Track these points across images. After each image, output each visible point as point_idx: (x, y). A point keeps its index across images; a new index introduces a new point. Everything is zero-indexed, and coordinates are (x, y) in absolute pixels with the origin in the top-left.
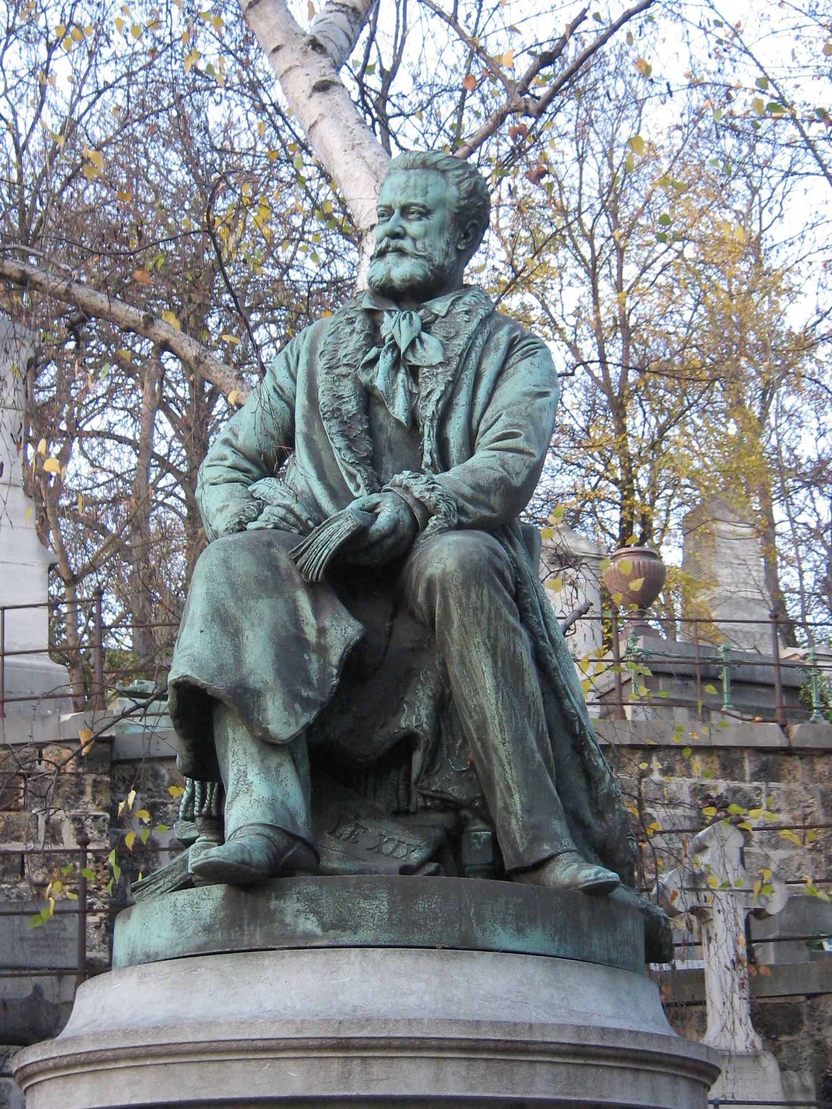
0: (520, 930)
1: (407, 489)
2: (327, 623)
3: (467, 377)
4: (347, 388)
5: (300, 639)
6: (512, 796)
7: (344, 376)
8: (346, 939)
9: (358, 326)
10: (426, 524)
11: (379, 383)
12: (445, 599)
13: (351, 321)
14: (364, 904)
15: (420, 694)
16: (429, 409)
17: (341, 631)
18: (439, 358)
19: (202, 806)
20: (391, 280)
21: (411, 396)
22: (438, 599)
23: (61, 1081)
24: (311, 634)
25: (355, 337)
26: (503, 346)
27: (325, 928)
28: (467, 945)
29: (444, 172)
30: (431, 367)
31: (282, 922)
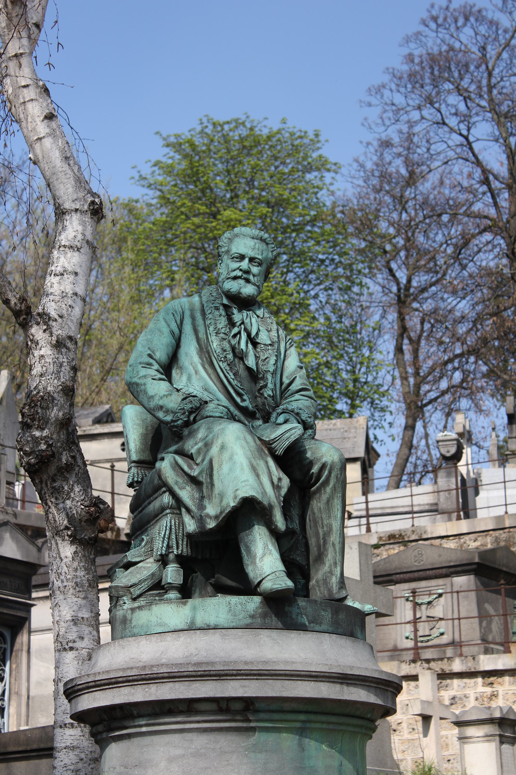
6: (336, 567)
8: (317, 628)
9: (223, 313)
13: (217, 309)
14: (323, 613)
15: (293, 512)
18: (269, 342)
19: (178, 548)
20: (240, 293)
22: (326, 473)
23: (187, 683)
29: (267, 244)
30: (265, 345)
31: (291, 617)
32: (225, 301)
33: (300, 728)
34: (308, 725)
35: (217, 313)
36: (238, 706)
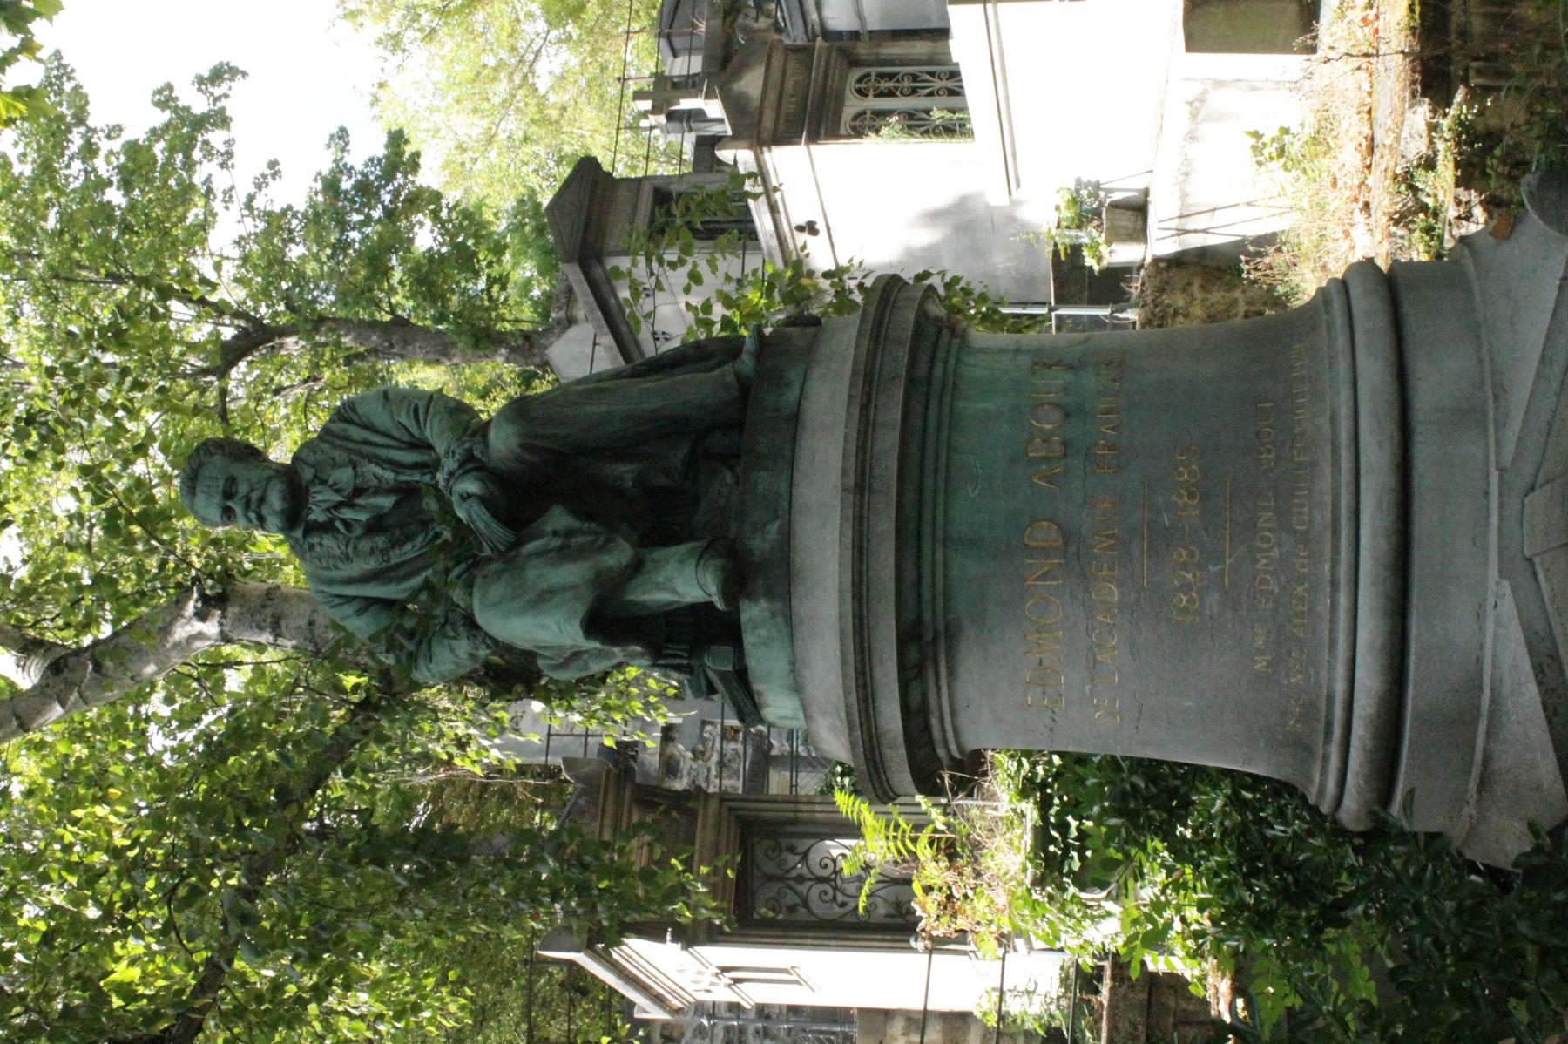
0: (787, 385)
1: (451, 474)
2: (549, 529)
3: (365, 449)
4: (365, 545)
5: (560, 549)
7: (355, 548)
9: (316, 540)
10: (479, 461)
11: (363, 517)
12: (536, 436)
13: (312, 547)
14: (761, 488)
16: (389, 475)
17: (559, 518)
18: (350, 470)
20: (283, 511)
21: (377, 492)
22: (537, 442)
24: (556, 542)
25: (325, 542)
26: (345, 426)
27: (775, 518)
28: (794, 419)
32: (299, 533)
33: (945, 546)
34: (940, 533)
35: (318, 548)
36: (913, 654)
